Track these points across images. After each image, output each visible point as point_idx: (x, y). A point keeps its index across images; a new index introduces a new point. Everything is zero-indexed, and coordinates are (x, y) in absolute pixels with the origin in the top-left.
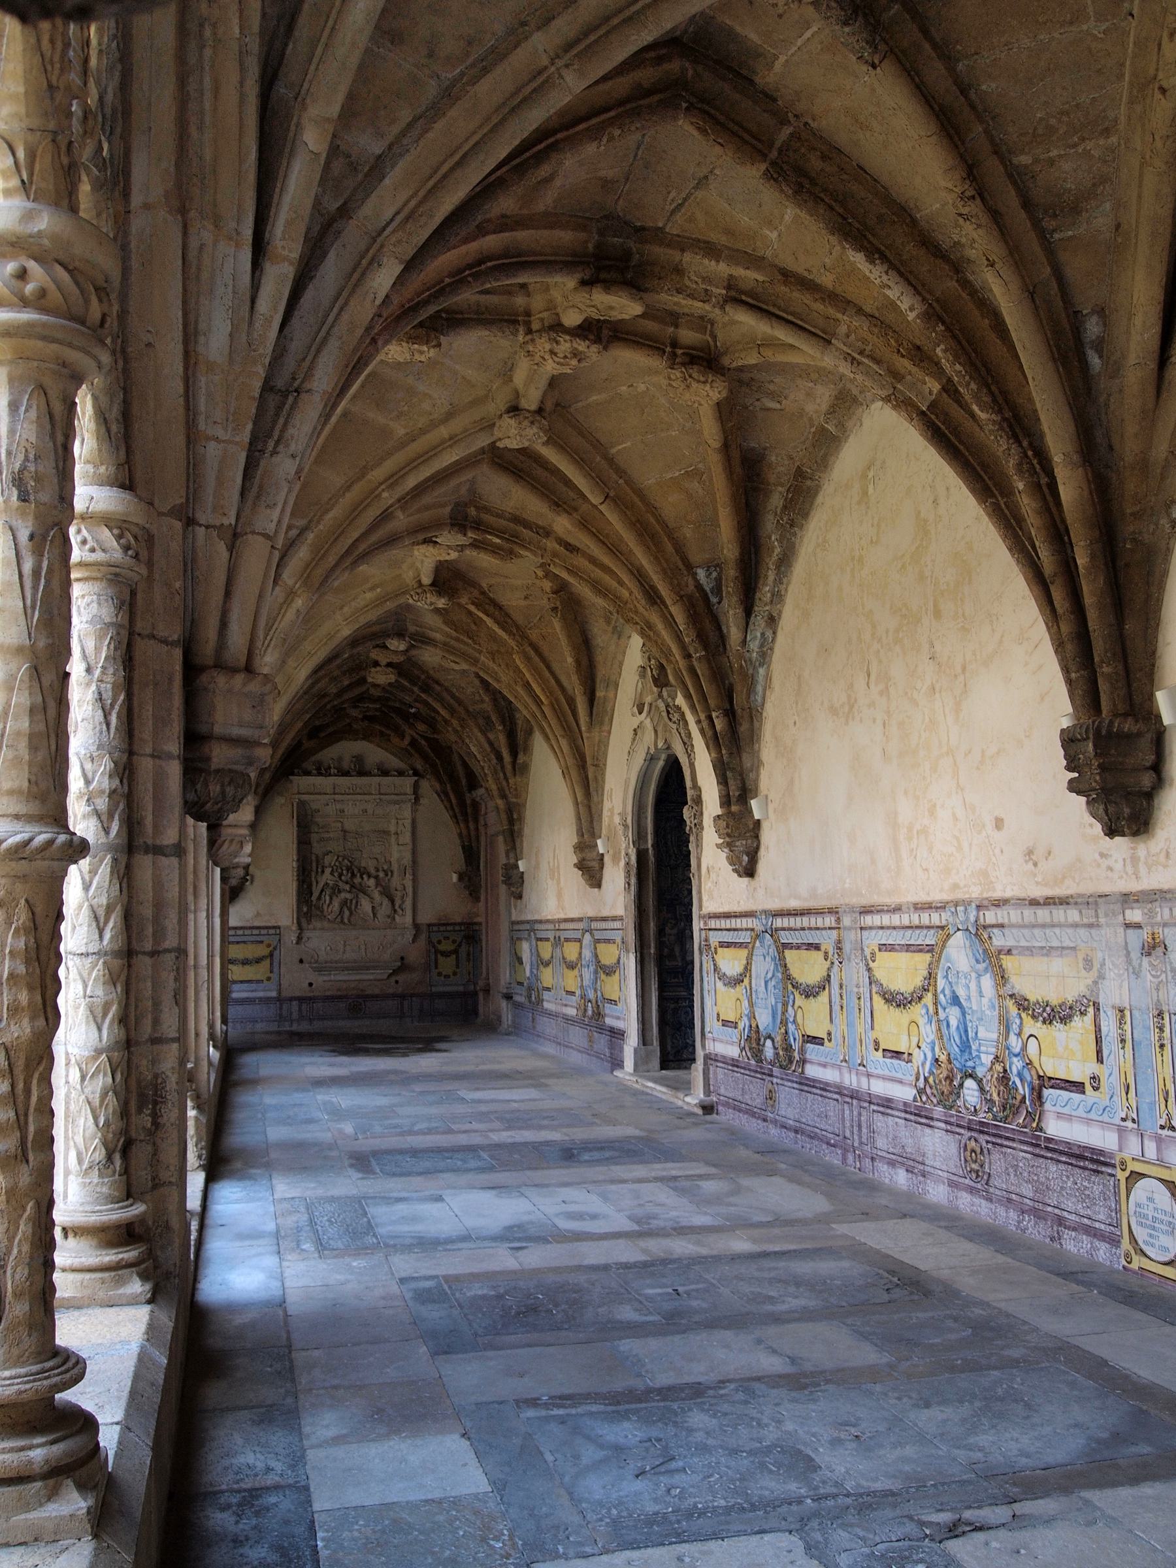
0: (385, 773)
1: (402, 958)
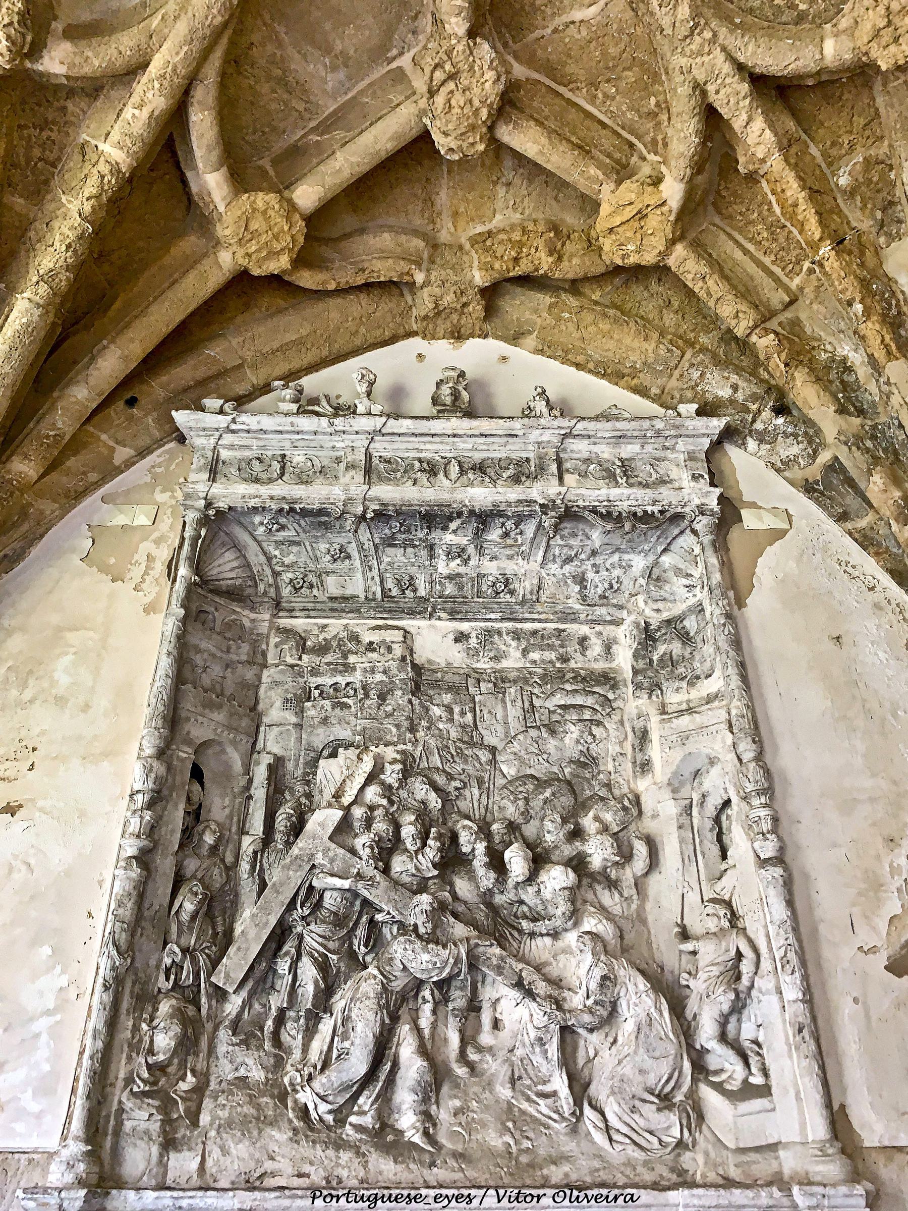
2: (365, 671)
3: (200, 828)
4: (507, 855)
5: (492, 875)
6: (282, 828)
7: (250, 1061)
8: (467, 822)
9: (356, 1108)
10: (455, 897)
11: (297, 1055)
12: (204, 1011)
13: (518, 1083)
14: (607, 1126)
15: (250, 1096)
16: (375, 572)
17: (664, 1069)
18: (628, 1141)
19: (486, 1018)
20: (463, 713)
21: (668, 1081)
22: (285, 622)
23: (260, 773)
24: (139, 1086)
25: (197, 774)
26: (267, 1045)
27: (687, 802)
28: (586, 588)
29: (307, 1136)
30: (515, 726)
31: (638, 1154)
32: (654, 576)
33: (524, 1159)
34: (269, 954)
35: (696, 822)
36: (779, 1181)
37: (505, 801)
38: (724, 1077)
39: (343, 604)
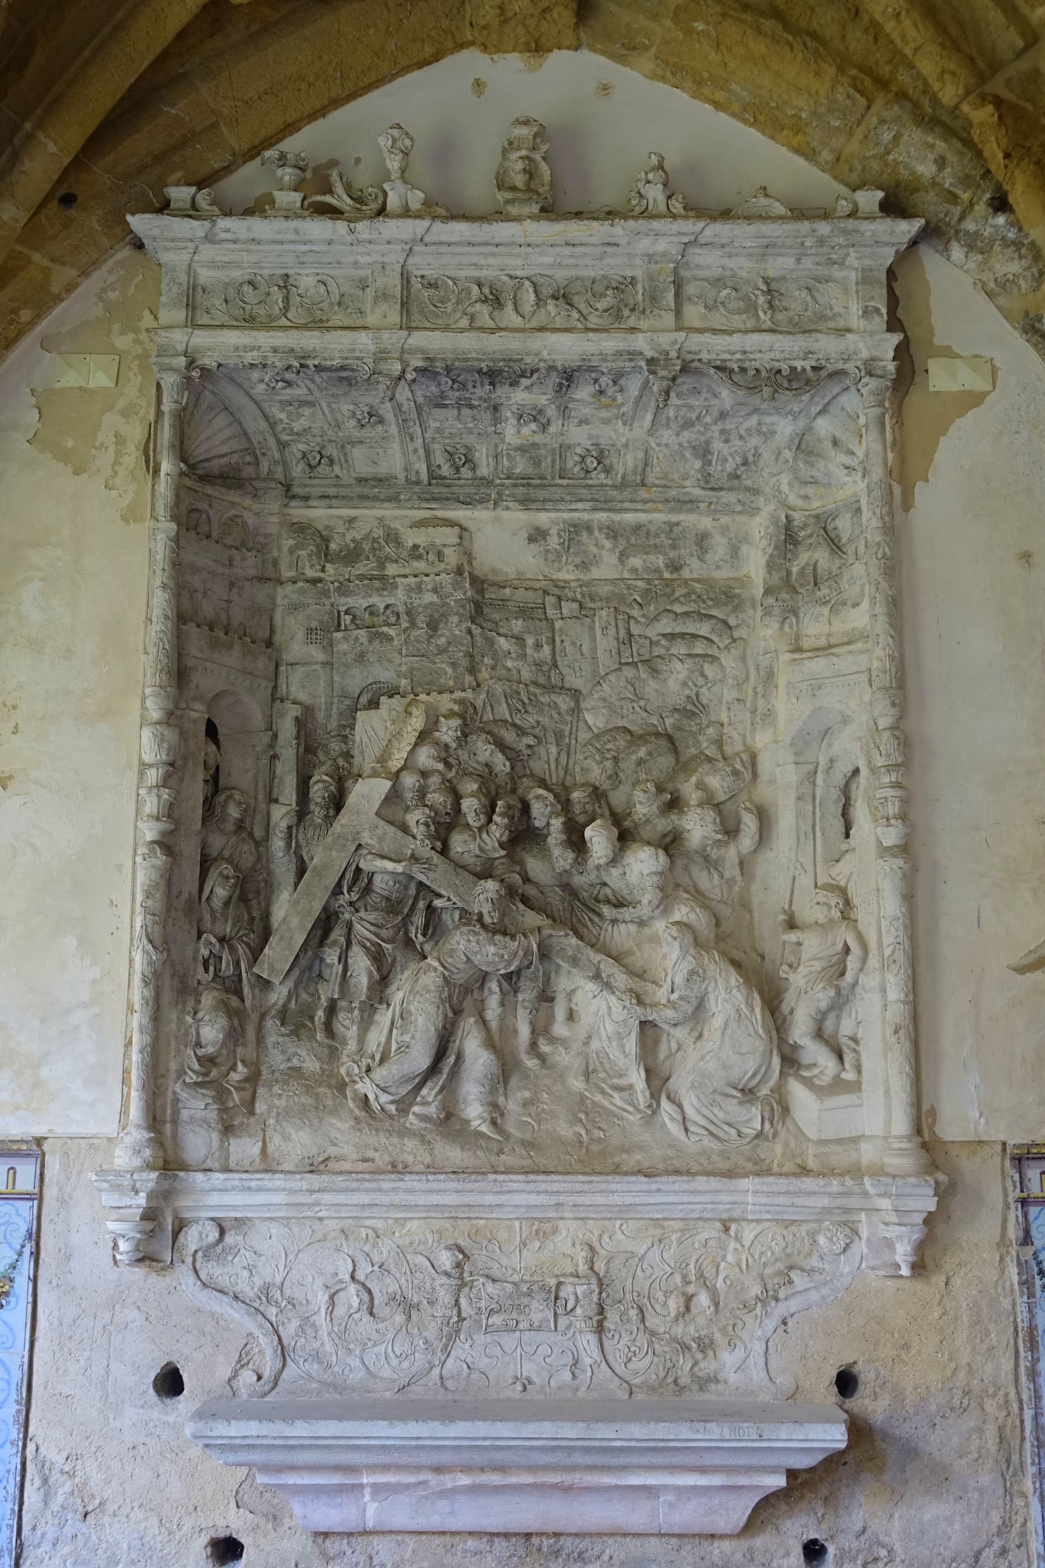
0: (709, 208)
1: (846, 1382)
2: (409, 590)
3: (222, 798)
4: (588, 833)
5: (571, 855)
6: (319, 800)
7: (303, 1052)
8: (541, 791)
9: (419, 1099)
10: (527, 879)
11: (352, 1046)
12: (248, 1003)
13: (591, 1076)
14: (684, 1118)
15: (306, 1086)
16: (419, 442)
17: (751, 1064)
18: (704, 1132)
19: (560, 1011)
20: (538, 646)
21: (753, 1076)
22: (299, 512)
23: (287, 728)
24: (191, 1078)
25: (211, 731)
26: (320, 1036)
27: (811, 767)
28: (710, 463)
29: (369, 1125)
30: (605, 663)
31: (715, 1145)
32: (804, 447)
33: (595, 1148)
34: (314, 943)
35: (819, 792)
36: (856, 1172)
37: (588, 761)
38: (815, 1071)
39: (375, 488)
